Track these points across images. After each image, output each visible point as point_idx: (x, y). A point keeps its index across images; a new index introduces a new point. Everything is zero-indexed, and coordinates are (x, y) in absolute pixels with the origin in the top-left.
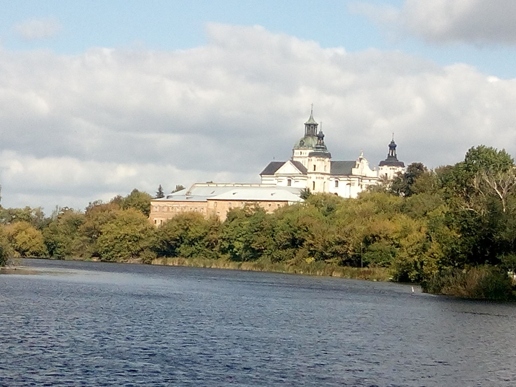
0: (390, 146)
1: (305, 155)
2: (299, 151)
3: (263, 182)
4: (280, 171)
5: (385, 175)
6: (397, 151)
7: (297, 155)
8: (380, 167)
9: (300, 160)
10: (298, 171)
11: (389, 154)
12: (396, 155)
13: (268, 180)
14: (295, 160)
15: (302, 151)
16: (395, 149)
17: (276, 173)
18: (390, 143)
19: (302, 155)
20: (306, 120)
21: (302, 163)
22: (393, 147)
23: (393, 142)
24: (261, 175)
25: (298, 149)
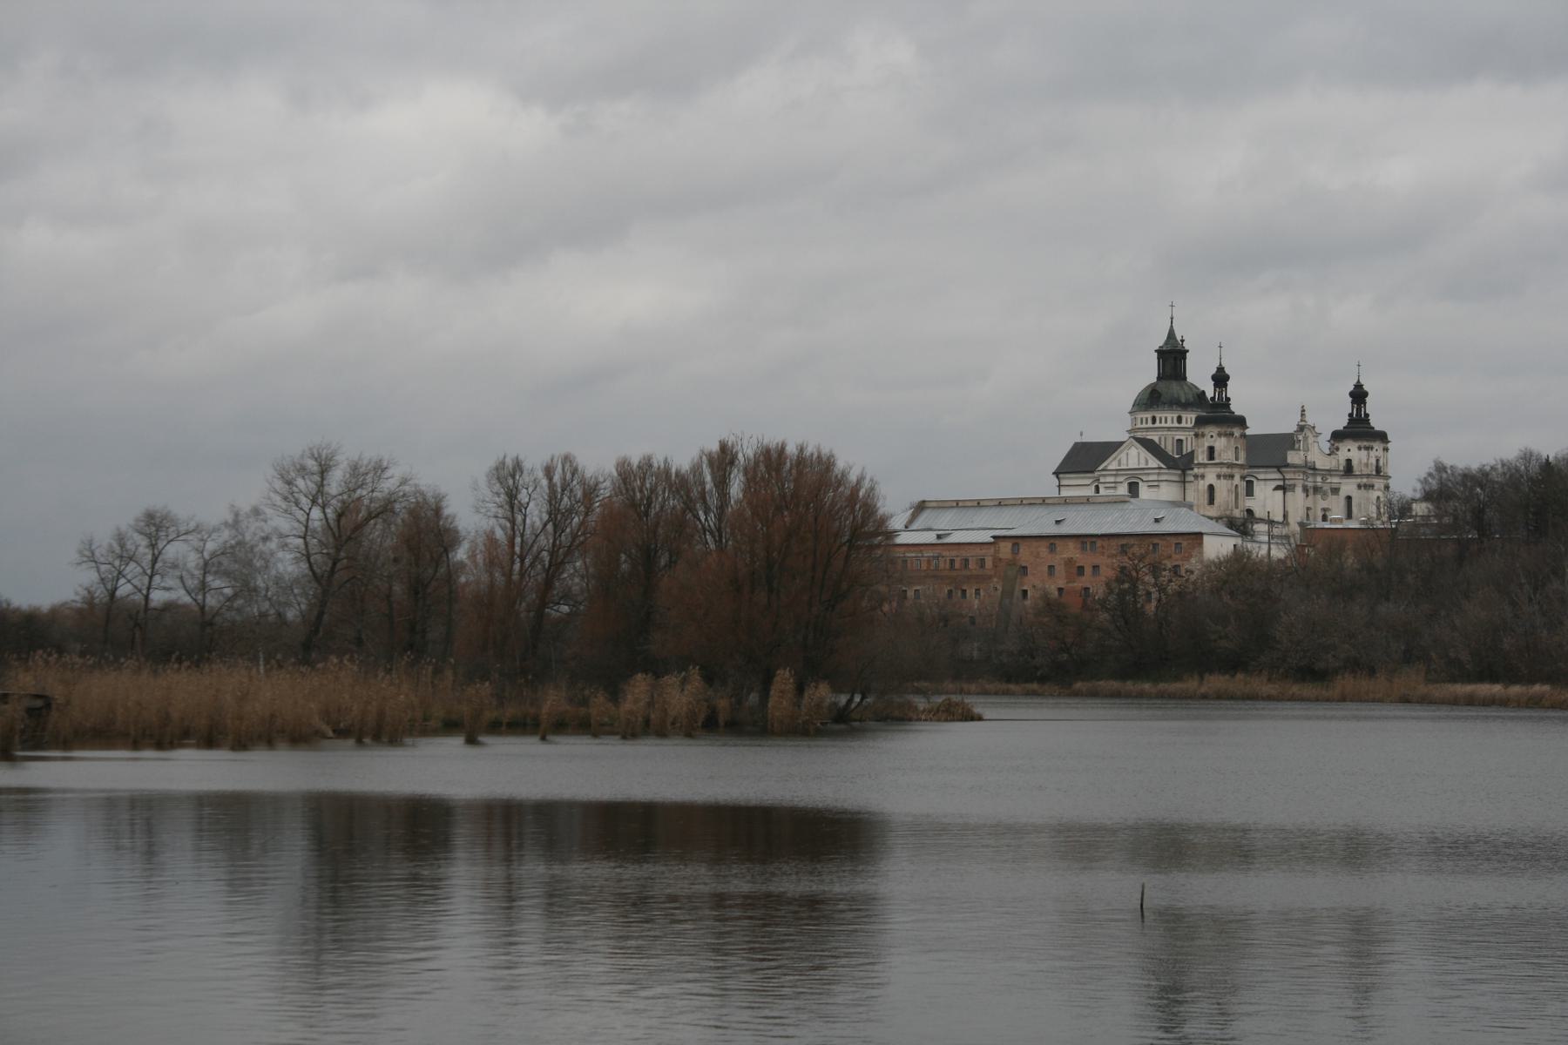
0: (1351, 394)
2: (1149, 415)
3: (1065, 493)
4: (1112, 464)
6: (1371, 406)
9: (1154, 437)
10: (1154, 462)
11: (1351, 415)
12: (1367, 415)
13: (1079, 487)
14: (1139, 435)
18: (1352, 388)
20: (1160, 341)
22: (1359, 395)
23: (1359, 386)
24: (1057, 473)
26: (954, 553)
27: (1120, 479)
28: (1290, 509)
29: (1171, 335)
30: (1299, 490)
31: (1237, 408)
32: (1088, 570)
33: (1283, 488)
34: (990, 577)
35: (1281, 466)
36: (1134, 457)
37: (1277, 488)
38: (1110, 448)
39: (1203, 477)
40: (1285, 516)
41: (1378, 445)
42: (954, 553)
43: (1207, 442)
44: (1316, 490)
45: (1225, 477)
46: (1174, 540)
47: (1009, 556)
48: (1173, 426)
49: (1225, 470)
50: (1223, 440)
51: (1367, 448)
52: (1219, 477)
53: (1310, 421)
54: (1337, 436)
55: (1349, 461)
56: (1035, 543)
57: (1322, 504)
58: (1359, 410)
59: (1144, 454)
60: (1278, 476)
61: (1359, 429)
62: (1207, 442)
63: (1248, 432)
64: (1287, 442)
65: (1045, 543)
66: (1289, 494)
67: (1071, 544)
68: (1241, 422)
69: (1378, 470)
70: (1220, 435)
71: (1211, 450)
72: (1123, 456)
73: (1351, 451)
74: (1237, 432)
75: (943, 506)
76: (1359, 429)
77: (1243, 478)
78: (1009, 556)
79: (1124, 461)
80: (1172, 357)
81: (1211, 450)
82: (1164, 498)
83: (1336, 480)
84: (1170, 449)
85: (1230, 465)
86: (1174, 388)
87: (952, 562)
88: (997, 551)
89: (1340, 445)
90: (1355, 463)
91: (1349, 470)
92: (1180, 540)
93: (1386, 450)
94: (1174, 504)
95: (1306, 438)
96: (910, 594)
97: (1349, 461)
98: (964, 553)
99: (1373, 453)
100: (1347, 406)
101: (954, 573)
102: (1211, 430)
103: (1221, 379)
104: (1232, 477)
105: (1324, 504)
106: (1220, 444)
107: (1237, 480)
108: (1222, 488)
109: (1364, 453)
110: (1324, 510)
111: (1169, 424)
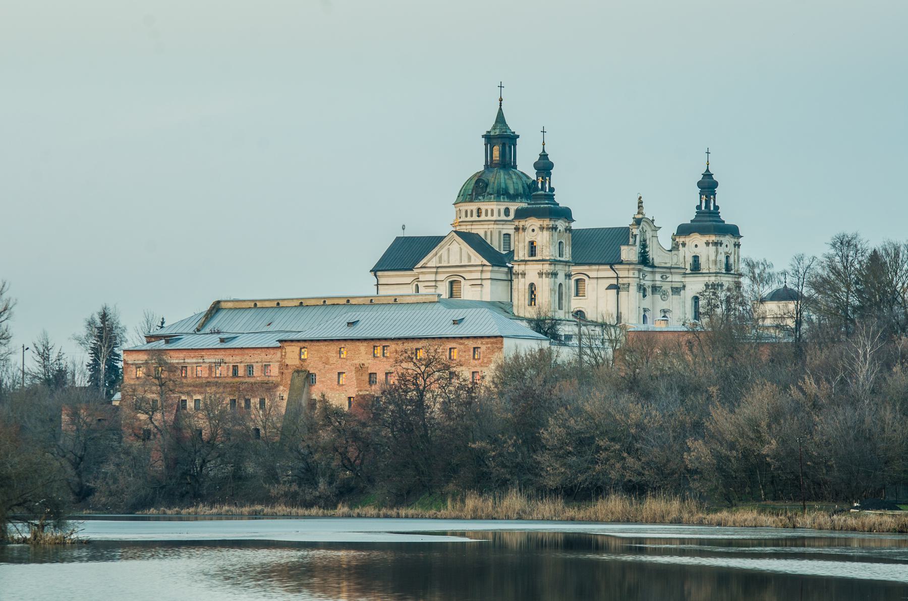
0: (699, 184)
1: (489, 217)
2: (473, 206)
3: (383, 291)
4: (431, 260)
5: (690, 260)
6: (721, 198)
7: (469, 219)
8: (680, 240)
9: (479, 230)
10: (477, 259)
11: (699, 207)
12: (716, 208)
13: (398, 284)
14: (464, 229)
15: (485, 206)
16: (715, 195)
17: (419, 265)
19: (483, 217)
20: (488, 124)
21: (483, 237)
22: (708, 186)
23: (708, 175)
25: (471, 201)
26: (238, 359)
27: (440, 277)
28: (624, 310)
29: (500, 119)
30: (633, 289)
31: (561, 199)
32: (381, 377)
33: (616, 288)
34: (276, 386)
35: (614, 261)
36: (457, 253)
37: (611, 287)
38: (432, 243)
39: (524, 274)
40: (619, 318)
41: (727, 240)
42: (238, 359)
43: (528, 236)
44: (655, 289)
45: (547, 274)
46: (471, 344)
47: (297, 362)
48: (492, 218)
49: (547, 268)
50: (546, 234)
51: (716, 244)
52: (541, 274)
53: (648, 213)
54: (684, 230)
55: (696, 258)
56: (323, 347)
57: (662, 305)
58: (708, 203)
59: (467, 249)
60: (611, 274)
61: (709, 222)
62: (528, 236)
63: (574, 226)
64: (622, 236)
65: (334, 347)
66: (623, 294)
67: (363, 347)
68: (566, 214)
69: (728, 268)
70: (542, 228)
71: (532, 243)
72: (444, 252)
73: (698, 245)
74: (561, 224)
75: (240, 307)
76: (709, 222)
77: (568, 276)
78: (297, 362)
79: (445, 257)
80: (502, 141)
81: (532, 243)
82: (487, 298)
83: (677, 278)
84: (496, 244)
85: (554, 262)
86: (500, 178)
87: (235, 368)
88: (283, 357)
89: (687, 240)
90: (702, 261)
91: (696, 267)
92: (478, 343)
93: (737, 245)
94: (493, 305)
95: (643, 232)
96: (190, 404)
97: (696, 258)
98: (248, 359)
99: (722, 249)
100: (694, 197)
101: (237, 380)
102: (533, 223)
103: (544, 166)
104: (555, 274)
105: (664, 305)
106: (543, 239)
107: (561, 278)
108: (544, 288)
109: (712, 248)
110: (665, 311)
111: (495, 217)
